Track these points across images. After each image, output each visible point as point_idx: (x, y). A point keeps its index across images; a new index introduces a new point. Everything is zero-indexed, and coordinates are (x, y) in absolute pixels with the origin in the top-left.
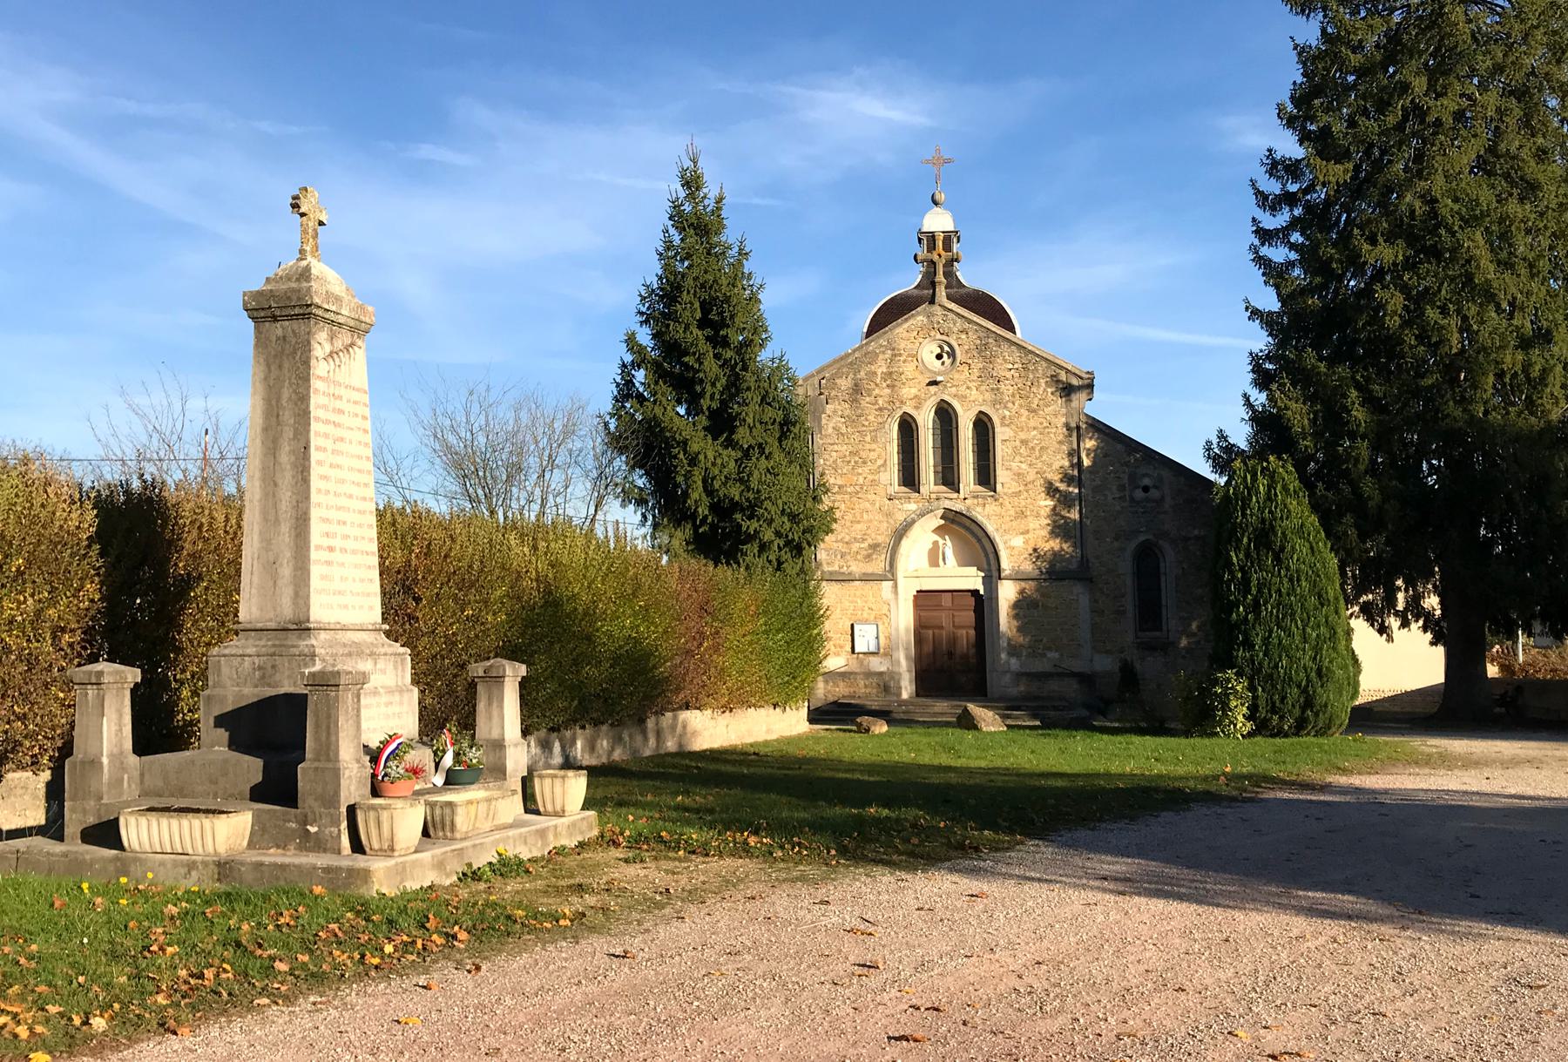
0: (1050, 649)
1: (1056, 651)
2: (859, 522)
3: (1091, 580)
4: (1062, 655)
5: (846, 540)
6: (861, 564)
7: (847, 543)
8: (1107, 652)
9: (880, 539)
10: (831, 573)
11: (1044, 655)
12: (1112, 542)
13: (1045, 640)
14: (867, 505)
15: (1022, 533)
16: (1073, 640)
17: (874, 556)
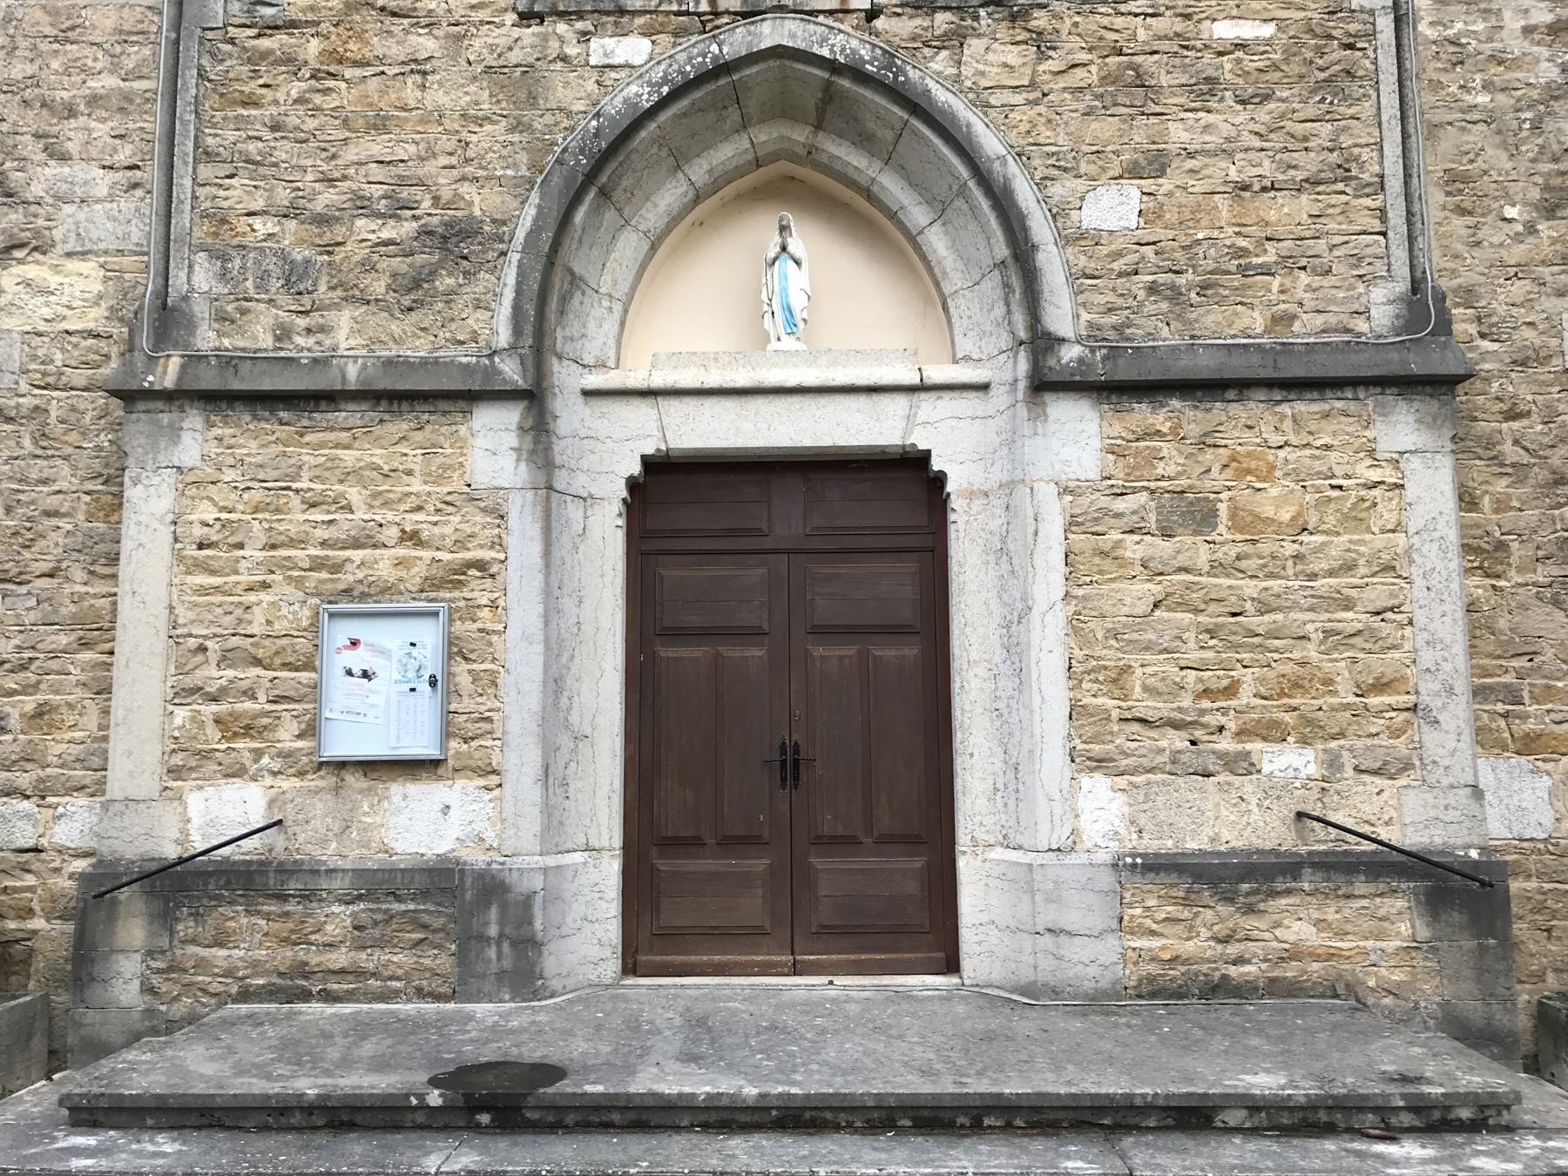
0: (1272, 732)
1: (1304, 741)
2: (379, 125)
3: (1441, 385)
4: (1333, 763)
5: (319, 206)
6: (379, 321)
7: (322, 220)
8: (1528, 745)
9: (481, 202)
10: (228, 362)
11: (1241, 765)
12: (1531, 229)
13: (1245, 697)
14: (425, 44)
15: (1133, 172)
16: (1380, 686)
17: (446, 282)
